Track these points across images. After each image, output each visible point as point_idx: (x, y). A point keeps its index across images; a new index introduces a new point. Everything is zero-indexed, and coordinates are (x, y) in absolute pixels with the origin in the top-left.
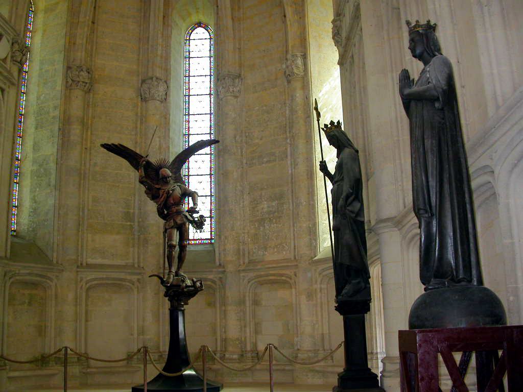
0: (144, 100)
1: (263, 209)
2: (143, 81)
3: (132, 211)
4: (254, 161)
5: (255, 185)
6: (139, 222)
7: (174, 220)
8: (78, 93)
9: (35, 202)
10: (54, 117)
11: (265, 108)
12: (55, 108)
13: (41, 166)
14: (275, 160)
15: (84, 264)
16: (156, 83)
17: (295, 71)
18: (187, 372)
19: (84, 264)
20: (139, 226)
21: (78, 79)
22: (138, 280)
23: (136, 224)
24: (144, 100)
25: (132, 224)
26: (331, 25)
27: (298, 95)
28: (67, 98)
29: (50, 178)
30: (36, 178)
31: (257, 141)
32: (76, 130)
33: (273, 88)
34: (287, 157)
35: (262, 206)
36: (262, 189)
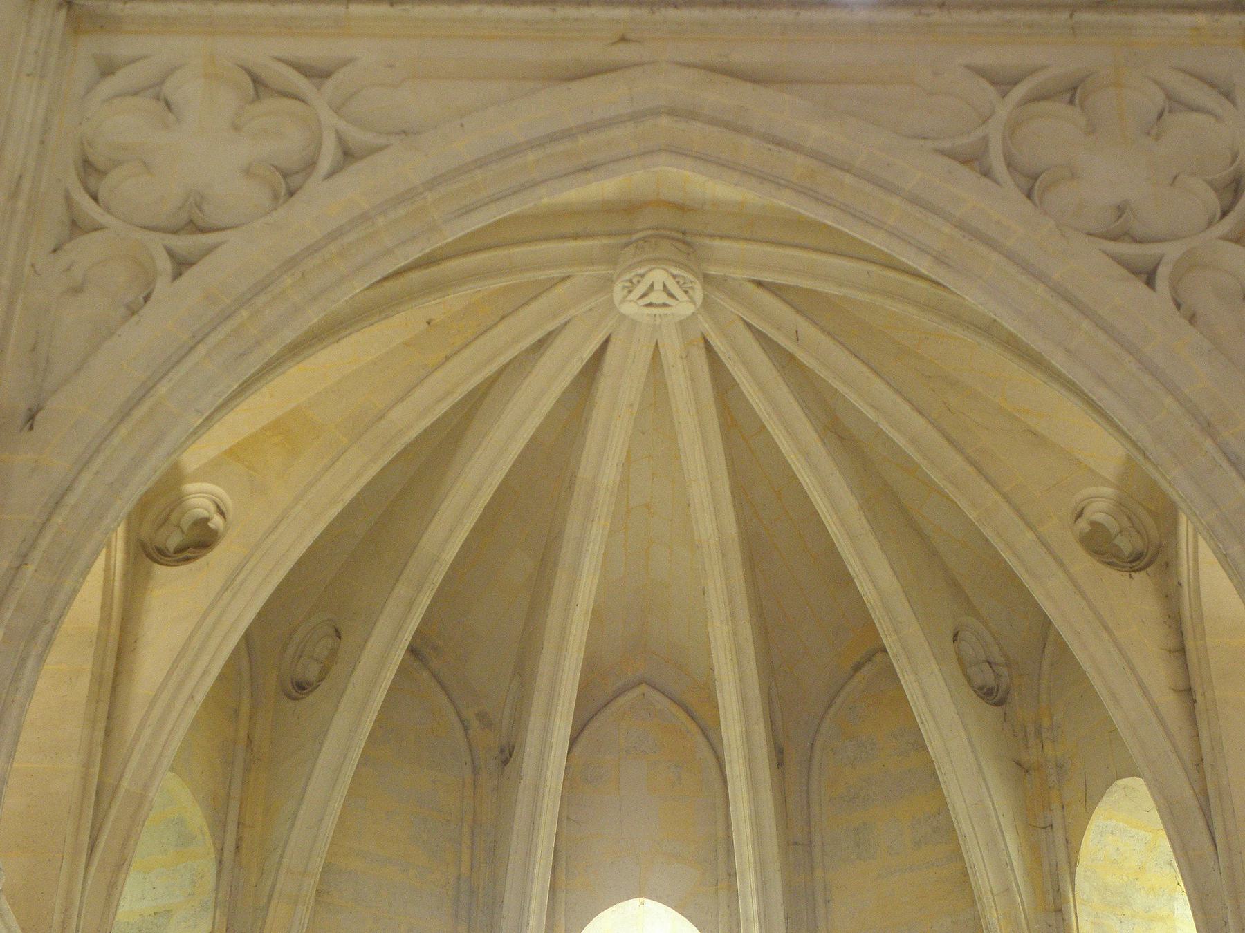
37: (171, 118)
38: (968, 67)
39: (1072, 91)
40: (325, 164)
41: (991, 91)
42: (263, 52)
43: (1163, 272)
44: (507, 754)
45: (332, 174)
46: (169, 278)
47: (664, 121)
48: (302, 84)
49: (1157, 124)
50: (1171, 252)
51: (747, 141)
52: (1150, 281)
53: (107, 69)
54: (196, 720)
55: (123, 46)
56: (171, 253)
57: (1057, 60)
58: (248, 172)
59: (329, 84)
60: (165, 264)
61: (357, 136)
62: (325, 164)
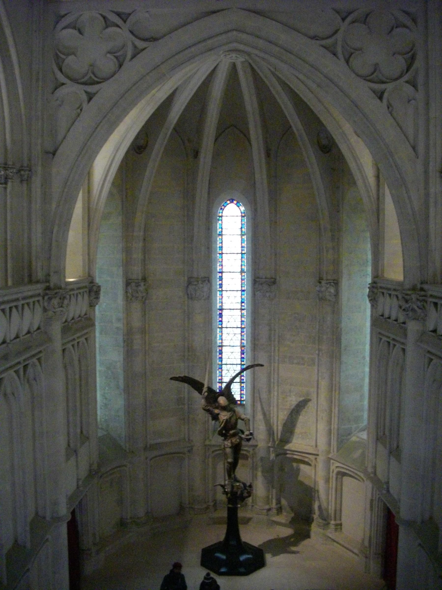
0: (190, 297)
1: (291, 400)
2: (189, 283)
3: (182, 396)
4: (286, 360)
5: (286, 380)
6: (189, 404)
7: (231, 440)
8: (136, 306)
9: (106, 399)
10: (118, 328)
11: (297, 315)
12: (119, 320)
13: (108, 368)
14: (304, 364)
15: (148, 446)
16: (201, 285)
17: (328, 297)
18: (243, 558)
19: (148, 446)
20: (188, 407)
21: (137, 295)
22: (189, 451)
23: (186, 407)
24: (190, 297)
25: (183, 406)
26: (368, 290)
27: (329, 319)
28: (128, 311)
29: (118, 382)
30: (104, 378)
31: (288, 343)
32: (137, 339)
33: (306, 300)
34: (314, 363)
35: (291, 399)
36: (291, 385)
38: (333, 9)
43: (386, 95)
44: (196, 154)
46: (86, 103)
47: (235, 33)
50: (390, 87)
51: (261, 41)
52: (381, 98)
54: (111, 194)
56: (86, 92)
60: (85, 97)
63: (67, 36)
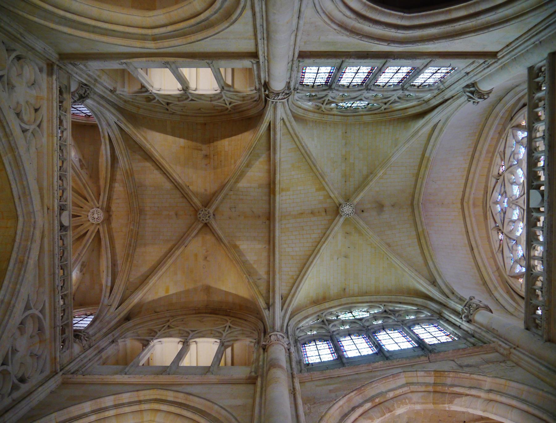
37: (30, 85)
39: (41, 329)
40: (23, 125)
41: (40, 308)
42: (44, 111)
45: (20, 126)
48: (38, 122)
49: (32, 355)
53: (41, 70)
55: (45, 76)
57: (47, 324)
58: (18, 103)
59: (37, 128)
61: (29, 134)
62: (23, 125)
63: (30, 71)
